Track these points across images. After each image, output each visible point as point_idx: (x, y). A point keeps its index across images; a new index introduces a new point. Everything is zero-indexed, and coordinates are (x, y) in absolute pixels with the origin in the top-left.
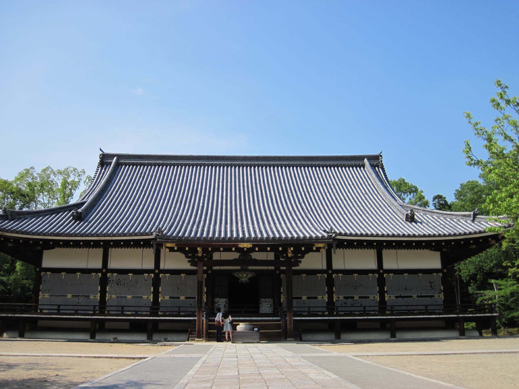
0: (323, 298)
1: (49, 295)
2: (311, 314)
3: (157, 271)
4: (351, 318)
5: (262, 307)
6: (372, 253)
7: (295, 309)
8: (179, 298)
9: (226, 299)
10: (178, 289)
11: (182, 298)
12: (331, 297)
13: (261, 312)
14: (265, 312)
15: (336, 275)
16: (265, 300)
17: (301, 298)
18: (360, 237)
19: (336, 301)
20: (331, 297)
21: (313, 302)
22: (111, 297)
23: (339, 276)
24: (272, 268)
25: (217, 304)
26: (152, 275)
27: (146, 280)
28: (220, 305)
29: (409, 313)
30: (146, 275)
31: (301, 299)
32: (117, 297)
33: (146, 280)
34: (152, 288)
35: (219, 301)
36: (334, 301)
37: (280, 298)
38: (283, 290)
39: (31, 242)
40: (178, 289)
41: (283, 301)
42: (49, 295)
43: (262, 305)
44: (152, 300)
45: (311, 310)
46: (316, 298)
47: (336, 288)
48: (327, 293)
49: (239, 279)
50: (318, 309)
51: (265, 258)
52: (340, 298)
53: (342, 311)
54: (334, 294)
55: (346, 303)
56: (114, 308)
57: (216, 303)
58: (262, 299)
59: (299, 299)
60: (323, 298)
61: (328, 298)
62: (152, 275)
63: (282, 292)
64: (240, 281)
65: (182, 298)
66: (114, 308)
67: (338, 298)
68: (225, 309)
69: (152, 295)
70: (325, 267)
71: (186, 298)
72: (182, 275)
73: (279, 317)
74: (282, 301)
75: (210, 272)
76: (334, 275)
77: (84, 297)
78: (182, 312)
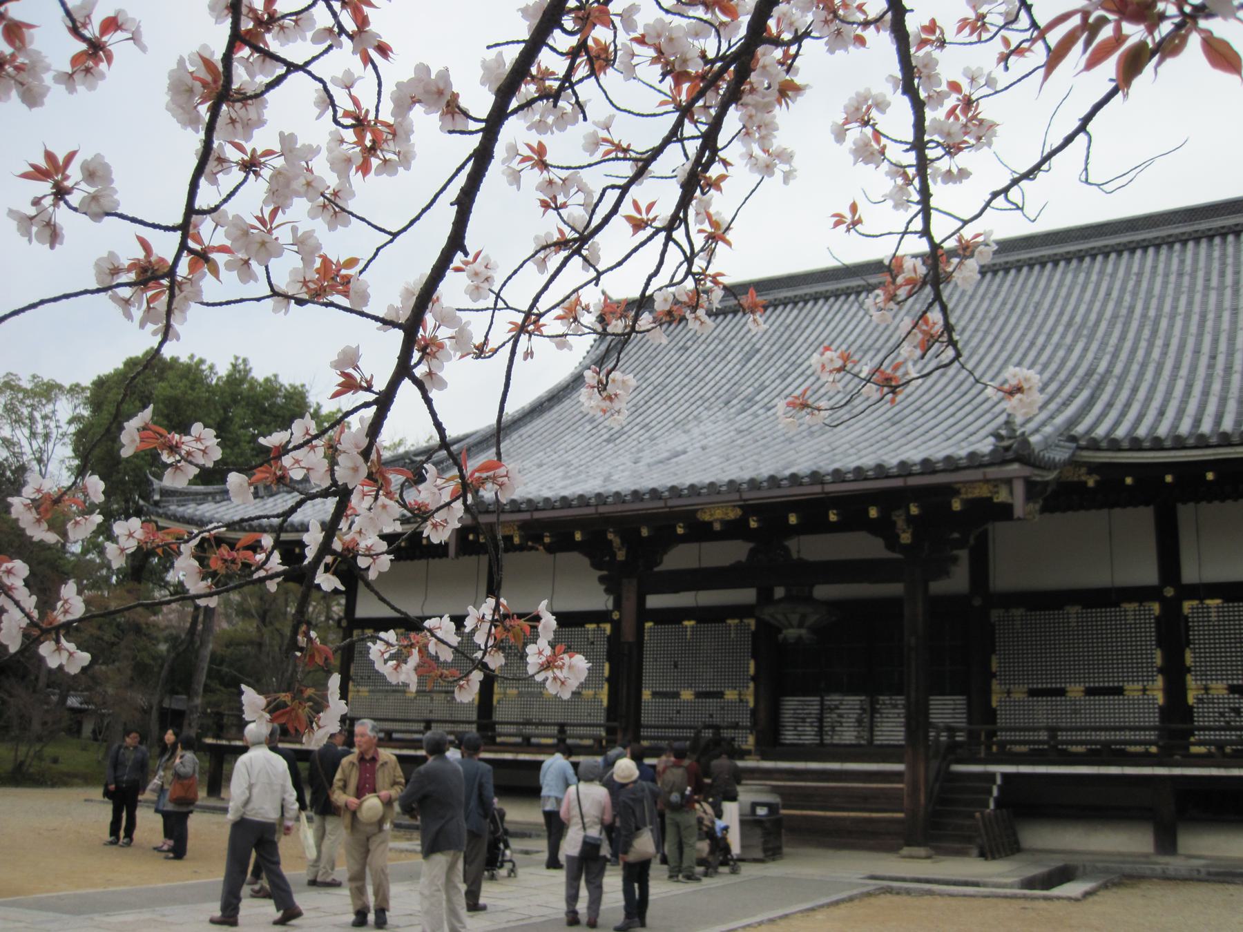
0: (1144, 690)
1: (369, 691)
2: (1112, 750)
3: (1169, 592)
4: (1214, 772)
5: (882, 722)
6: (1143, 518)
7: (1002, 736)
8: (676, 695)
9: (863, 698)
10: (676, 666)
11: (687, 695)
12: (1176, 690)
13: (878, 742)
14: (892, 742)
15: (1195, 603)
16: (891, 699)
17: (1061, 692)
18: (1172, 453)
19: (1197, 703)
20: (1176, 690)
21: (1104, 710)
22: (505, 694)
23: (1208, 607)
24: (895, 589)
25: (835, 716)
26: (1156, 608)
27: (592, 643)
28: (843, 717)
29: (1121, 757)
30: (591, 627)
31: (1124, 695)
32: (520, 694)
33: (592, 643)
34: (607, 666)
35: (842, 704)
36: (1191, 700)
37: (987, 693)
38: (1000, 663)
39: (645, 532)
40: (676, 666)
41: (1000, 701)
42: (369, 691)
43: (882, 717)
44: (605, 703)
45: (1062, 736)
46: (1119, 691)
47: (1195, 653)
48: (1161, 671)
49: (779, 631)
50: (1128, 735)
51: (693, 565)
52: (1211, 692)
53: (1200, 743)
54: (1189, 678)
55: (1237, 711)
56: (512, 729)
57: (831, 709)
58: (881, 698)
59: (1114, 694)
60: (1144, 690)
61: (1183, 690)
62: (1156, 608)
63: (994, 669)
64: (781, 637)
65: (687, 695)
66: (512, 729)
67: (1206, 689)
68: (858, 731)
69: (606, 686)
70: (1148, 574)
71: (698, 695)
72: (686, 623)
73: (900, 762)
74: (994, 704)
75: (977, 602)
76: (1187, 606)
77: (443, 695)
78: (646, 738)
